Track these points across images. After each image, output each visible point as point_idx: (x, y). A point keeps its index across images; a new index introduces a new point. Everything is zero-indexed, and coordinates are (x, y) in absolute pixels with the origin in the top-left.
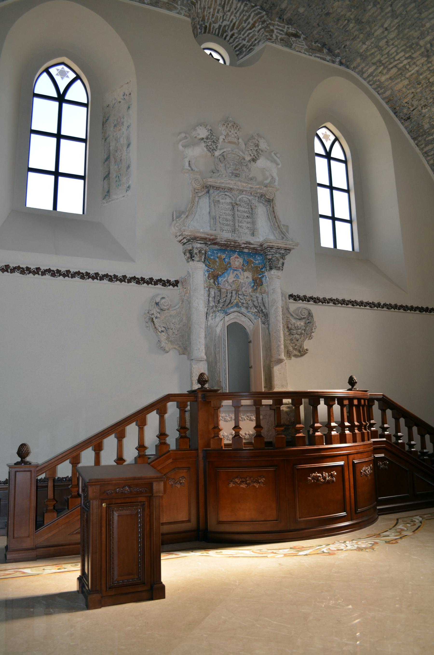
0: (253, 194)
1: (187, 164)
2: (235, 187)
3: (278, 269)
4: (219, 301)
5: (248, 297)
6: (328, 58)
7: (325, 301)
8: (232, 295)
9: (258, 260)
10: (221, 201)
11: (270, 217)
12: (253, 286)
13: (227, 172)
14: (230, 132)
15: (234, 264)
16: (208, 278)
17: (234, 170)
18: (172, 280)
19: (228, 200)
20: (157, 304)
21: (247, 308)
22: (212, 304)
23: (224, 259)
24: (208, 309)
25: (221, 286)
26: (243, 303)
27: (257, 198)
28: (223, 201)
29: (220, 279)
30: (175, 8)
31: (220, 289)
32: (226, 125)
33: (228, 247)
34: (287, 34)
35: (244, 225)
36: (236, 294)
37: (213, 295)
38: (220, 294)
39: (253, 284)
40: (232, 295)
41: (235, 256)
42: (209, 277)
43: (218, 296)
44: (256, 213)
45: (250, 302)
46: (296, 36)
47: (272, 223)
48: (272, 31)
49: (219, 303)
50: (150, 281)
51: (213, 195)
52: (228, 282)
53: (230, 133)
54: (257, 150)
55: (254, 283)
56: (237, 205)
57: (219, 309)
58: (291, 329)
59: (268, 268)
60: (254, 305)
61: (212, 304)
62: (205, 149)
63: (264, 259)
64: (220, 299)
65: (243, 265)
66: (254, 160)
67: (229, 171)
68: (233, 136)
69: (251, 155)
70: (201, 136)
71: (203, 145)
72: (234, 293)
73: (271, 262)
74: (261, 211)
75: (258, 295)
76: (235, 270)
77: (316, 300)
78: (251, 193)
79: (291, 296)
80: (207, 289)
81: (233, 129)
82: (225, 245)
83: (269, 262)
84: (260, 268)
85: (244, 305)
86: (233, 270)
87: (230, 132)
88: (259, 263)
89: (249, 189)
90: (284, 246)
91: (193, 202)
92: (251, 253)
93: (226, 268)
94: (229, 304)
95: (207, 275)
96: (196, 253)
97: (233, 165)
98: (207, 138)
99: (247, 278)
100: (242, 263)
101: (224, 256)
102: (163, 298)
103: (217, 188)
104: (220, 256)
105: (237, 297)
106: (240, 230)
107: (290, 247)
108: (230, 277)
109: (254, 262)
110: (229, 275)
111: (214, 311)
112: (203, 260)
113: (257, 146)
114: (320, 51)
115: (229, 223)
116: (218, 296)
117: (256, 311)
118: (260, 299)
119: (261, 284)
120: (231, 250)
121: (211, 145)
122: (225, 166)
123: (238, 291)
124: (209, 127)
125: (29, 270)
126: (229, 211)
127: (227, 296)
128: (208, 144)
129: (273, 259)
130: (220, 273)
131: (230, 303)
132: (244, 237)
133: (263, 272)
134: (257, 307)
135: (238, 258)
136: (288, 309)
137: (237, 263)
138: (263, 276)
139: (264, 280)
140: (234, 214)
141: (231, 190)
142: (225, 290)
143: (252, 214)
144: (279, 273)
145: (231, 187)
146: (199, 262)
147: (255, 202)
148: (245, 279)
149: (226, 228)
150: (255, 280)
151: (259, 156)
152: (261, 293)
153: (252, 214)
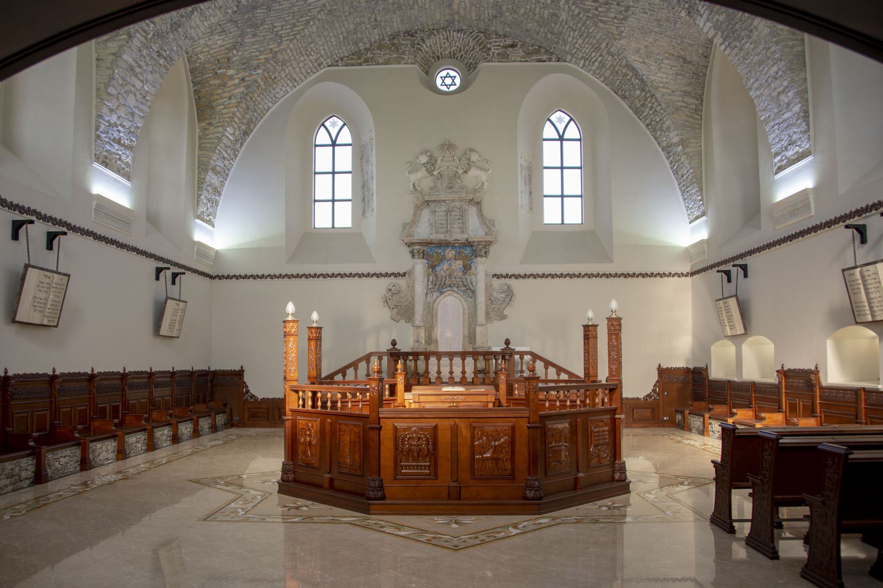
1: (411, 186)
3: (482, 256)
6: (544, 57)
7: (525, 276)
9: (468, 251)
18: (401, 272)
19: (443, 208)
22: (430, 286)
30: (404, 59)
34: (504, 47)
35: (456, 225)
45: (460, 283)
46: (513, 46)
48: (490, 49)
50: (387, 275)
61: (430, 286)
63: (472, 250)
66: (466, 172)
67: (444, 185)
71: (424, 169)
74: (472, 211)
77: (517, 277)
79: (494, 276)
91: (415, 215)
93: (442, 259)
103: (434, 201)
106: (453, 230)
113: (469, 159)
114: (537, 52)
124: (429, 154)
125: (310, 276)
132: (458, 236)
136: (491, 285)
137: (450, 255)
139: (472, 265)
141: (445, 201)
143: (463, 216)
144: (484, 259)
147: (465, 207)
150: (464, 266)
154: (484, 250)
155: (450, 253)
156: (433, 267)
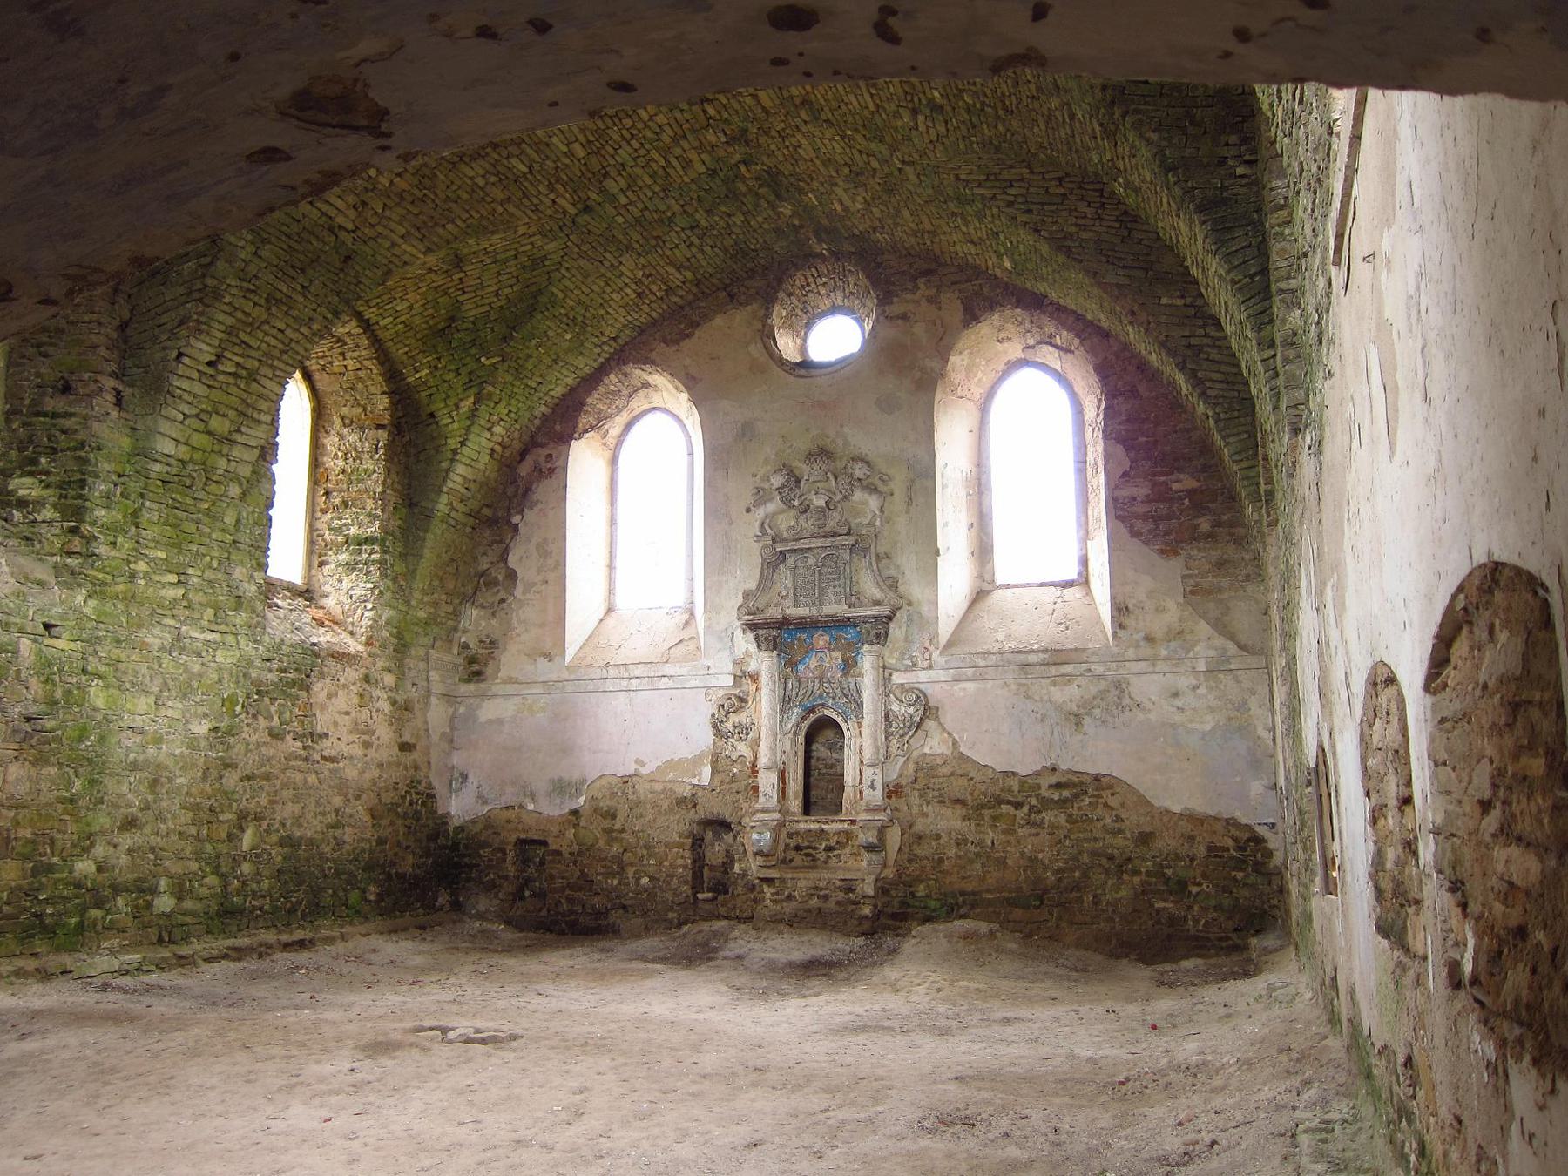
3: (871, 643)
45: (838, 691)
66: (846, 498)
93: (809, 650)
101: (804, 636)
144: (876, 647)
150: (845, 661)
155: (821, 640)
156: (791, 664)
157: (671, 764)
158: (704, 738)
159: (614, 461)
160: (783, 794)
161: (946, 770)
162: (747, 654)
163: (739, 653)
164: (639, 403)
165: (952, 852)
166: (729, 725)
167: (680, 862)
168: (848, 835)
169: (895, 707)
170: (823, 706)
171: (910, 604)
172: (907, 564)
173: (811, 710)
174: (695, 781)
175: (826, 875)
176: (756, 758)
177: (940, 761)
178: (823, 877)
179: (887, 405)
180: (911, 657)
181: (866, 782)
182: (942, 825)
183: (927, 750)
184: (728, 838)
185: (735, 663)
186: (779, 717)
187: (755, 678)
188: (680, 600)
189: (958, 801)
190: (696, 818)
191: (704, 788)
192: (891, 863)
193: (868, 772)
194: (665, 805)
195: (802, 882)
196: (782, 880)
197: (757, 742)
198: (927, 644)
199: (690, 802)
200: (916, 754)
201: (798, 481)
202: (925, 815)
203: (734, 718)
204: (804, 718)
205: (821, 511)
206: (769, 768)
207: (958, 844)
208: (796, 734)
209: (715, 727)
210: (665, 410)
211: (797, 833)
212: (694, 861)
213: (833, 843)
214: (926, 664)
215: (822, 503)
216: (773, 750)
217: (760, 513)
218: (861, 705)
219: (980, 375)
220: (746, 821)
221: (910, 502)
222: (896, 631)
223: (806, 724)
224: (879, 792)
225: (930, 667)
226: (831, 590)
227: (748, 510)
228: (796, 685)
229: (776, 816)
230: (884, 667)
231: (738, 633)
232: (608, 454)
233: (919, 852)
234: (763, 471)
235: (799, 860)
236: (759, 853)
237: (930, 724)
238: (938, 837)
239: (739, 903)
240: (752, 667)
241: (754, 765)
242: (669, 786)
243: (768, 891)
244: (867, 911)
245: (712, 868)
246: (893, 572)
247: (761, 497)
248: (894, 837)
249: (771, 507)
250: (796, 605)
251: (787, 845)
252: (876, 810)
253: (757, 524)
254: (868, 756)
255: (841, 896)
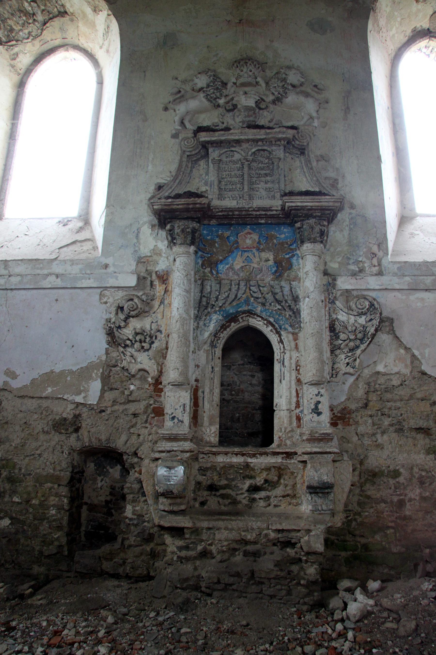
0: (274, 142)
2: (242, 137)
3: (314, 241)
4: (217, 298)
5: (265, 289)
8: (239, 288)
9: (284, 234)
10: (224, 159)
11: (305, 170)
12: (276, 272)
13: (235, 122)
14: (242, 71)
15: (245, 242)
16: (202, 267)
17: (245, 117)
20: (122, 308)
21: (263, 305)
23: (228, 237)
24: (198, 311)
25: (222, 276)
26: (258, 298)
27: (282, 147)
28: (228, 159)
29: (220, 267)
31: (220, 280)
32: (235, 65)
33: (232, 219)
36: (246, 285)
37: (209, 290)
38: (220, 287)
39: (274, 269)
40: (239, 288)
41: (246, 231)
42: (203, 265)
43: (216, 291)
44: (281, 168)
45: (269, 297)
47: (309, 178)
49: (217, 300)
51: (212, 154)
52: (233, 269)
53: (241, 73)
54: (284, 85)
55: (277, 267)
56: (248, 161)
57: (217, 309)
58: (339, 332)
59: (299, 242)
60: (276, 300)
62: (204, 100)
64: (219, 295)
65: (259, 243)
68: (246, 75)
69: (273, 94)
70: (199, 85)
72: (242, 284)
73: (302, 232)
75: (283, 283)
76: (246, 251)
78: (271, 141)
80: (199, 282)
81: (245, 66)
82: (225, 217)
83: (299, 233)
84: (287, 244)
85: (259, 300)
86: (242, 251)
87: (242, 71)
88: (286, 238)
89: (264, 137)
90: (317, 204)
92: (271, 224)
94: (233, 301)
95: (200, 263)
96: (177, 233)
97: (244, 111)
98: (208, 86)
99: (267, 260)
100: (257, 240)
102: (132, 300)
104: (222, 234)
105: (248, 290)
107: (326, 204)
108: (236, 262)
109: (278, 236)
110: (234, 260)
111: (209, 312)
112: (188, 242)
113: (284, 80)
115: (234, 187)
116: (216, 291)
117: (280, 307)
118: (287, 290)
119: (290, 266)
120: (239, 224)
121: (214, 93)
122: (234, 116)
123: (250, 281)
126: (236, 172)
127: (230, 290)
128: (209, 93)
129: (304, 227)
130: (221, 258)
131: (235, 299)
133: (292, 249)
134: (282, 302)
135: (250, 234)
137: (249, 242)
138: (293, 256)
139: (294, 260)
140: (243, 174)
142: (229, 281)
145: (237, 138)
146: (183, 245)
148: (262, 263)
149: (230, 194)
150: (278, 263)
151: (286, 93)
152: (289, 281)
153: (273, 170)
154: (317, 228)
155: (249, 238)
157: (50, 378)
158: (96, 346)
159: (21, 86)
160: (195, 418)
161: (404, 392)
162: (156, 252)
163: (145, 251)
164: (52, 34)
165: (414, 493)
166: (128, 332)
167: (53, 500)
168: (280, 471)
169: (342, 317)
170: (251, 313)
171: (352, 207)
172: (348, 168)
173: (233, 318)
174: (79, 399)
175: (256, 524)
176: (161, 373)
177: (396, 382)
178: (251, 526)
179: (319, 27)
180: (357, 262)
181: (307, 404)
182: (402, 458)
183: (380, 368)
184: (115, 472)
185: (141, 261)
186: (192, 325)
187: (164, 278)
188: (73, 210)
189: (419, 430)
190: (78, 445)
191: (91, 408)
192: (340, 507)
193: (309, 394)
194: (39, 426)
195: (224, 533)
196: (196, 531)
197: (163, 354)
198: (375, 249)
199: (72, 425)
200: (367, 372)
201: (225, 84)
202: (380, 447)
203: (135, 324)
204: (223, 327)
205: (248, 109)
206: (178, 385)
207: (422, 483)
208: (213, 345)
209: (110, 333)
210: (77, 48)
211: (213, 468)
212: (72, 500)
213: (259, 481)
214: (375, 270)
215: (251, 103)
216: (185, 360)
217: (182, 108)
218: (297, 313)
219: (394, 31)
220: (143, 451)
221: (347, 110)
222: (338, 233)
223: (225, 335)
224: (326, 417)
225: (380, 273)
226: (262, 185)
227: (166, 109)
228: (216, 287)
229: (187, 445)
230: (326, 273)
231: (146, 230)
232: (16, 78)
233: (371, 491)
234: (183, 76)
235: (213, 503)
236: (167, 494)
237: (384, 338)
238: (396, 474)
239: (130, 556)
240: (162, 265)
241: (158, 382)
242: (45, 404)
243: (172, 544)
244: (312, 571)
245: (92, 508)
246: (332, 174)
247: (180, 96)
248: (344, 477)
249: (193, 104)
250: (221, 197)
251: (199, 483)
252: (325, 438)
253: (177, 119)
254: (309, 373)
255: (278, 554)
